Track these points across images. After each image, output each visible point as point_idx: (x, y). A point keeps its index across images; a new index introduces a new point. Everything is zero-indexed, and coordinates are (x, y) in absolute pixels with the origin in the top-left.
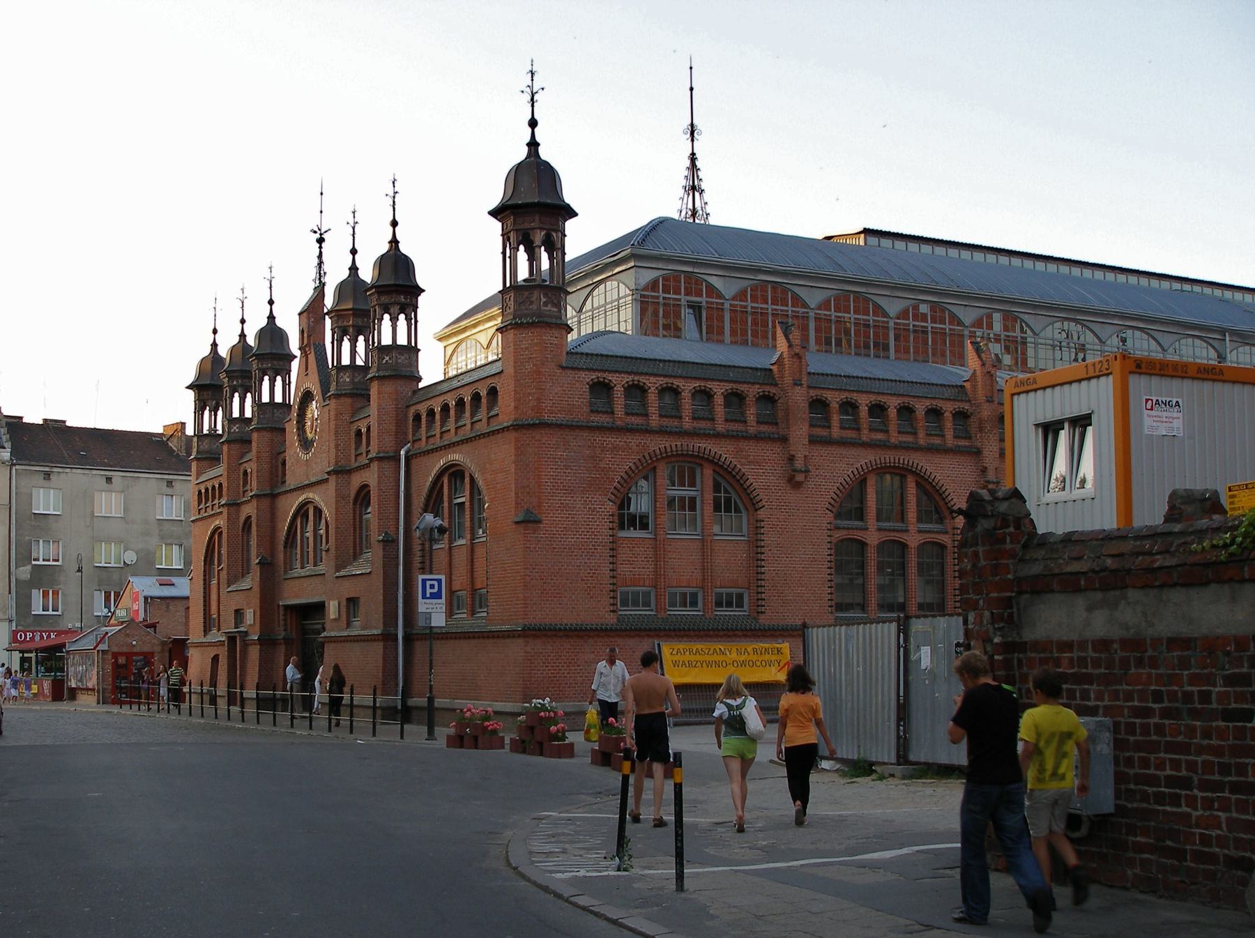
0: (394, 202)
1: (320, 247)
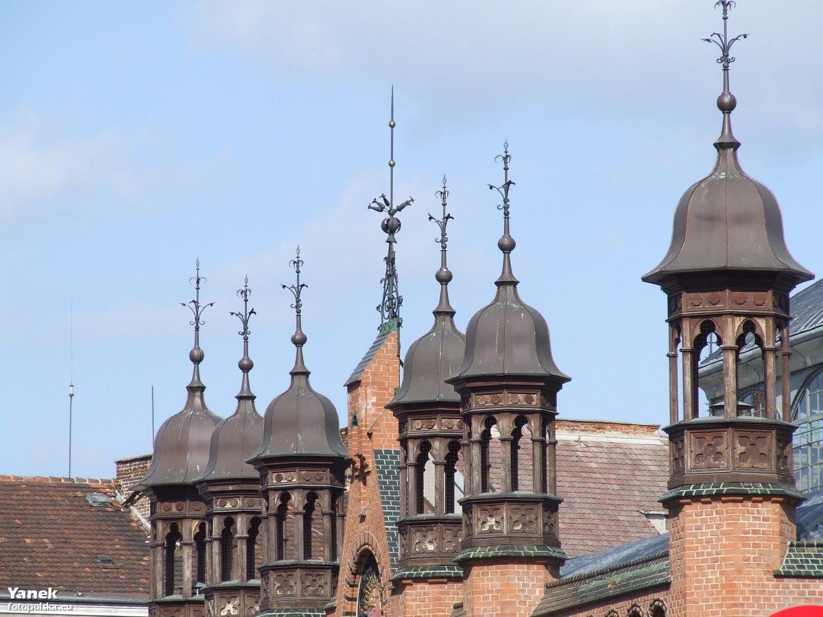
0: (506, 200)
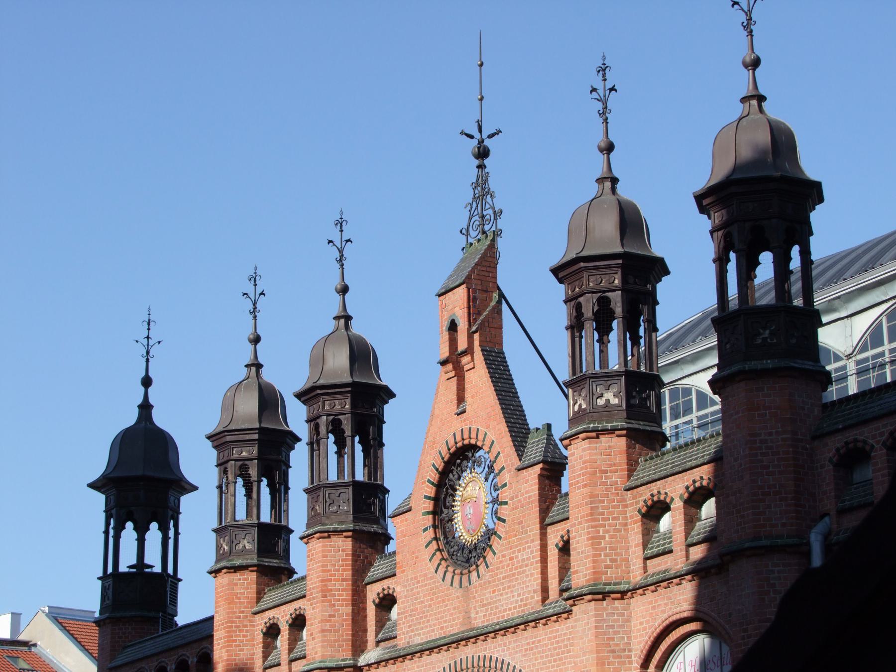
1: (481, 167)
